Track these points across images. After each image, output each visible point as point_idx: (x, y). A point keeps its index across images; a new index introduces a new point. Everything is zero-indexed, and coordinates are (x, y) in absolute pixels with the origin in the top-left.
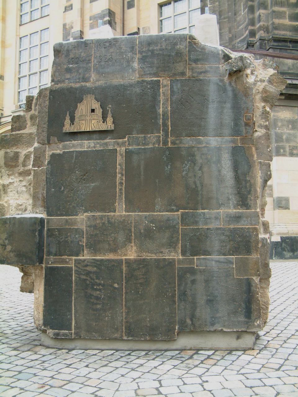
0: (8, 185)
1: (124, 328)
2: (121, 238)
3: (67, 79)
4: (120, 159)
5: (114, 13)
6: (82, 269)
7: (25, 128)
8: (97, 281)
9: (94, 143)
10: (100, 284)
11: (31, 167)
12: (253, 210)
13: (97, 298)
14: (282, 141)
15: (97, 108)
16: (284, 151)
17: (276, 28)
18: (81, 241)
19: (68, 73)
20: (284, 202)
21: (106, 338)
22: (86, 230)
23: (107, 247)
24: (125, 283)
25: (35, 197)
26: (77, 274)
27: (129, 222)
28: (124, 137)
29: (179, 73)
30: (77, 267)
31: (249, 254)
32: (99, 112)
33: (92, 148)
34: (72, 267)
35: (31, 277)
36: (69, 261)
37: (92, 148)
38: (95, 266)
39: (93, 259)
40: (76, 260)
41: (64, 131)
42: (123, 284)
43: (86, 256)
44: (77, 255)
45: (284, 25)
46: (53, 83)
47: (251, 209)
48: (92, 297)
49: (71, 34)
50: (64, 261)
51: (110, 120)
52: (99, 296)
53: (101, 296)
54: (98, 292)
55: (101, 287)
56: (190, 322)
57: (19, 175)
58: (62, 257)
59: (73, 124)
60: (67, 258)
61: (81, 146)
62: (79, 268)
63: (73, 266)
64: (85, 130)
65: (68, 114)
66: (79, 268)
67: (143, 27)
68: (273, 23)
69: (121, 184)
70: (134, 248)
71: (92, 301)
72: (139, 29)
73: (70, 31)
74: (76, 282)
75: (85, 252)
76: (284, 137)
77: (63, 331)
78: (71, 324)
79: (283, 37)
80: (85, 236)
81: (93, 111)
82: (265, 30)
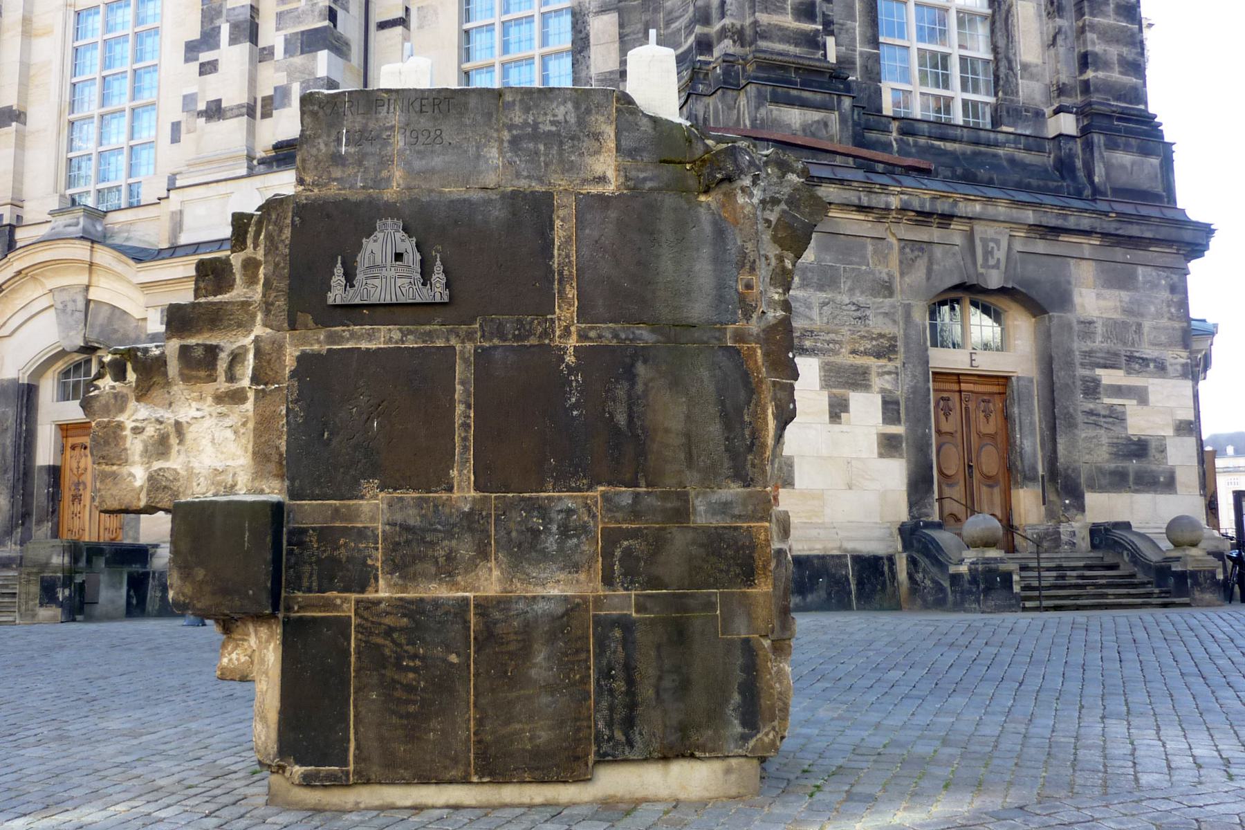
0: (188, 423)
1: (472, 756)
2: (465, 549)
3: (335, 180)
6: (372, 622)
7: (230, 286)
8: (409, 648)
9: (400, 330)
10: (415, 656)
11: (246, 382)
12: (759, 489)
13: (410, 689)
15: (410, 250)
17: (761, 33)
18: (370, 556)
19: (337, 165)
22: (384, 532)
23: (433, 570)
24: (475, 652)
25: (261, 456)
26: (362, 633)
27: (484, 513)
28: (472, 321)
29: (594, 178)
30: (362, 617)
31: (751, 585)
32: (413, 258)
33: (397, 343)
34: (350, 617)
35: (245, 643)
36: (343, 602)
37: (397, 343)
38: (404, 615)
39: (401, 599)
40: (358, 602)
41: (330, 301)
42: (469, 655)
43: (384, 591)
44: (363, 591)
45: (781, 28)
46: (301, 188)
47: (755, 486)
48: (398, 686)
49: (224, 12)
51: (438, 277)
52: (414, 683)
53: (419, 683)
54: (411, 675)
55: (418, 663)
56: (623, 739)
57: (157, 393)
58: (326, 594)
59: (352, 286)
60: (337, 597)
61: (370, 337)
62: (366, 620)
63: (353, 615)
64: (382, 302)
65: (339, 261)
66: (366, 620)
67: (420, 5)
68: (755, 23)
69: (465, 426)
70: (496, 573)
71: (397, 694)
72: (407, 9)
73: (221, 5)
74: (358, 652)
75: (381, 582)
77: (327, 768)
78: (347, 750)
79: (780, 58)
80: (380, 546)
81: (399, 257)
82: (736, 37)
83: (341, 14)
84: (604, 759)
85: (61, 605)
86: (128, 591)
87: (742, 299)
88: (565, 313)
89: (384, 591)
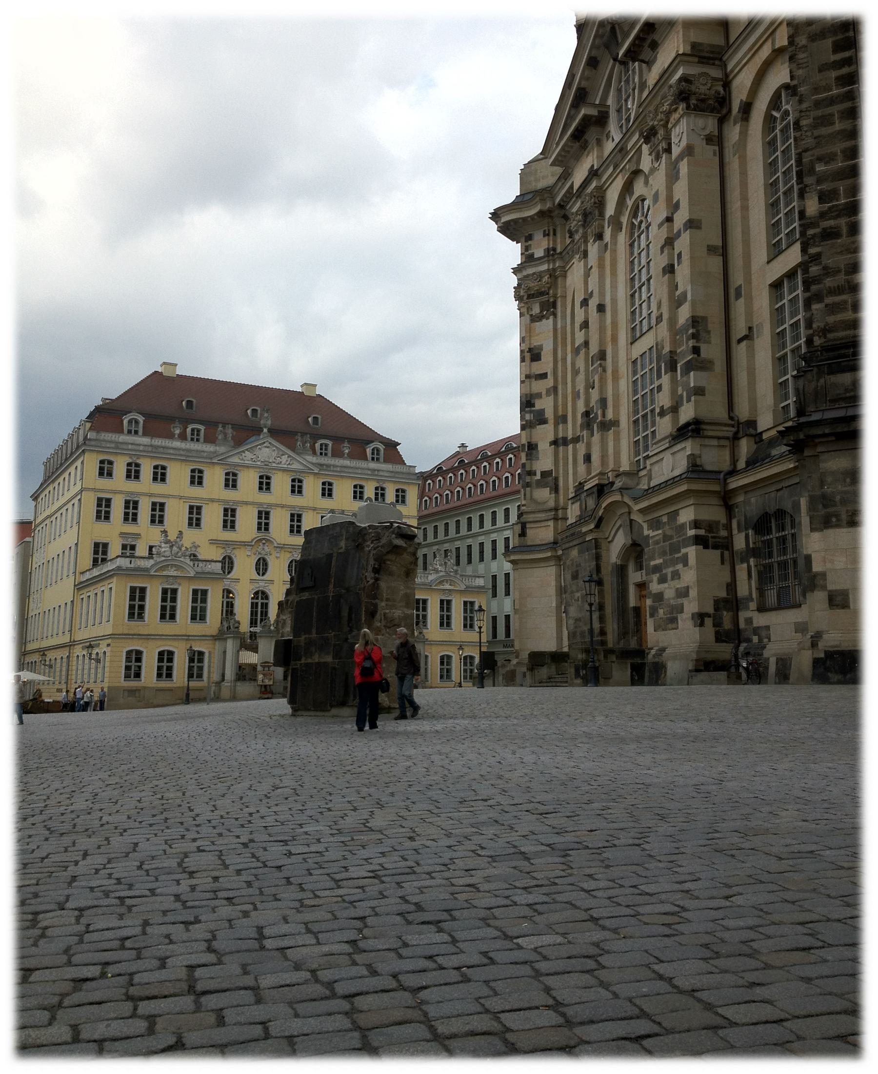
4: (315, 604)
5: (704, 319)
14: (835, 505)
16: (838, 520)
20: (839, 598)
21: (307, 709)
43: (303, 661)
45: (843, 322)
50: (296, 665)
72: (750, 329)
76: (838, 498)
83: (704, 348)
84: (332, 706)
85: (582, 678)
86: (631, 673)
87: (361, 579)
88: (331, 586)
89: (303, 661)
